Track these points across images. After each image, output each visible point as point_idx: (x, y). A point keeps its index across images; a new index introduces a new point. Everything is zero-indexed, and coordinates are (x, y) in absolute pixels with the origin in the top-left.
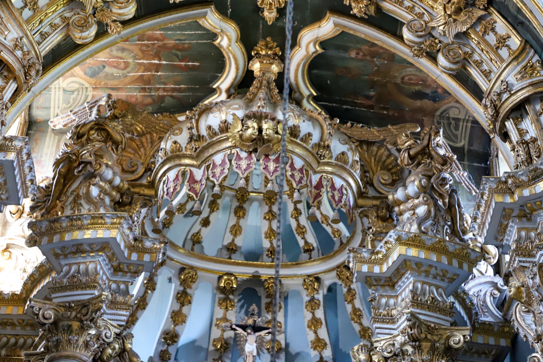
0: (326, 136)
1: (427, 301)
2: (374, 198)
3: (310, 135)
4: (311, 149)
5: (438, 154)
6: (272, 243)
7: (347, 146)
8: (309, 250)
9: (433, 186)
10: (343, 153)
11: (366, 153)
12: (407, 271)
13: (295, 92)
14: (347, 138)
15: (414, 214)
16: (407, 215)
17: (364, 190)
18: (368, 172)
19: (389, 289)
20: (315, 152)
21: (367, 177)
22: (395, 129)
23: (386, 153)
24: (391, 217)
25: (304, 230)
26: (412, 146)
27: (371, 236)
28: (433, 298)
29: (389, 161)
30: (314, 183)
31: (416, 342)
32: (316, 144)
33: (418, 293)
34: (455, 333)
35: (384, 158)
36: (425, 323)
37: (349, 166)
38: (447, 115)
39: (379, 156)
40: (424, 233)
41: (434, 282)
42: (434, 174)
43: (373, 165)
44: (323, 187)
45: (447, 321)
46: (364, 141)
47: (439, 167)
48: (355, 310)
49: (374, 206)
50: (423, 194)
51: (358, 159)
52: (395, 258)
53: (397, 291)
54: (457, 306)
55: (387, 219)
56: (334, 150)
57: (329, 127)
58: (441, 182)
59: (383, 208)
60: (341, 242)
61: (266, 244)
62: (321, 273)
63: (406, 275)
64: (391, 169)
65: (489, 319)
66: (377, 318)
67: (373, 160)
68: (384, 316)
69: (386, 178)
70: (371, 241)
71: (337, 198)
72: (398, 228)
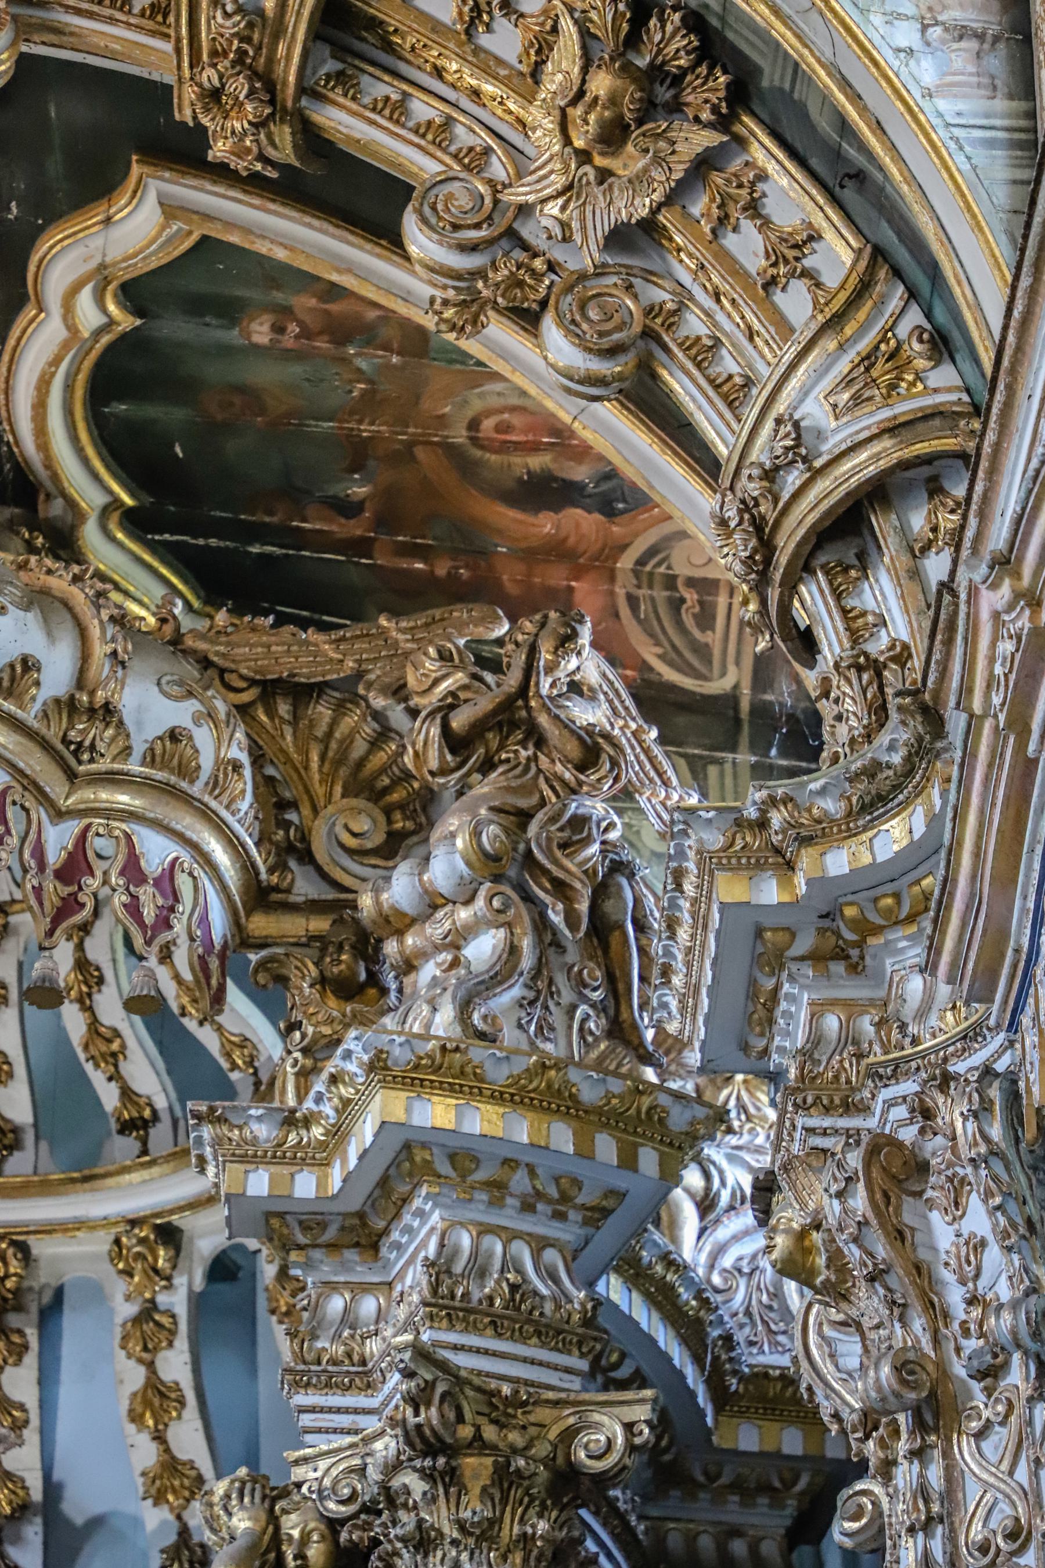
0: (100, 666)
1: (491, 1299)
2: (315, 907)
3: (28, 664)
4: (36, 725)
5: (567, 726)
7: (193, 705)
9: (529, 852)
10: (174, 735)
11: (288, 731)
12: (416, 1186)
13: (48, 496)
14: (190, 670)
15: (455, 963)
16: (429, 970)
17: (275, 879)
18: (294, 805)
19: (357, 1258)
20: (53, 733)
21: (286, 825)
22: (403, 631)
23: (369, 728)
24: (374, 979)
26: (462, 695)
27: (297, 1055)
28: (514, 1288)
29: (380, 758)
30: (54, 857)
31: (434, 1459)
32: (57, 701)
33: (458, 1268)
34: (596, 1417)
35: (360, 748)
36: (476, 1381)
37: (200, 784)
38: (662, 569)
39: (341, 742)
40: (482, 1036)
41: (526, 1224)
42: (543, 802)
43: (317, 777)
44: (92, 874)
45: (568, 1370)
46: (279, 680)
47: (567, 775)
49: (313, 938)
50: (489, 884)
51: (244, 758)
52: (369, 1139)
53: (387, 1266)
55: (361, 988)
56: (139, 724)
57: (111, 630)
58: (565, 834)
59: (340, 948)
60: (257, 1084)
63: (417, 1203)
64: (386, 791)
66: (303, 1373)
67: (315, 757)
68: (333, 1361)
69: (362, 824)
70: (297, 1075)
71: (149, 914)
72: (389, 1021)
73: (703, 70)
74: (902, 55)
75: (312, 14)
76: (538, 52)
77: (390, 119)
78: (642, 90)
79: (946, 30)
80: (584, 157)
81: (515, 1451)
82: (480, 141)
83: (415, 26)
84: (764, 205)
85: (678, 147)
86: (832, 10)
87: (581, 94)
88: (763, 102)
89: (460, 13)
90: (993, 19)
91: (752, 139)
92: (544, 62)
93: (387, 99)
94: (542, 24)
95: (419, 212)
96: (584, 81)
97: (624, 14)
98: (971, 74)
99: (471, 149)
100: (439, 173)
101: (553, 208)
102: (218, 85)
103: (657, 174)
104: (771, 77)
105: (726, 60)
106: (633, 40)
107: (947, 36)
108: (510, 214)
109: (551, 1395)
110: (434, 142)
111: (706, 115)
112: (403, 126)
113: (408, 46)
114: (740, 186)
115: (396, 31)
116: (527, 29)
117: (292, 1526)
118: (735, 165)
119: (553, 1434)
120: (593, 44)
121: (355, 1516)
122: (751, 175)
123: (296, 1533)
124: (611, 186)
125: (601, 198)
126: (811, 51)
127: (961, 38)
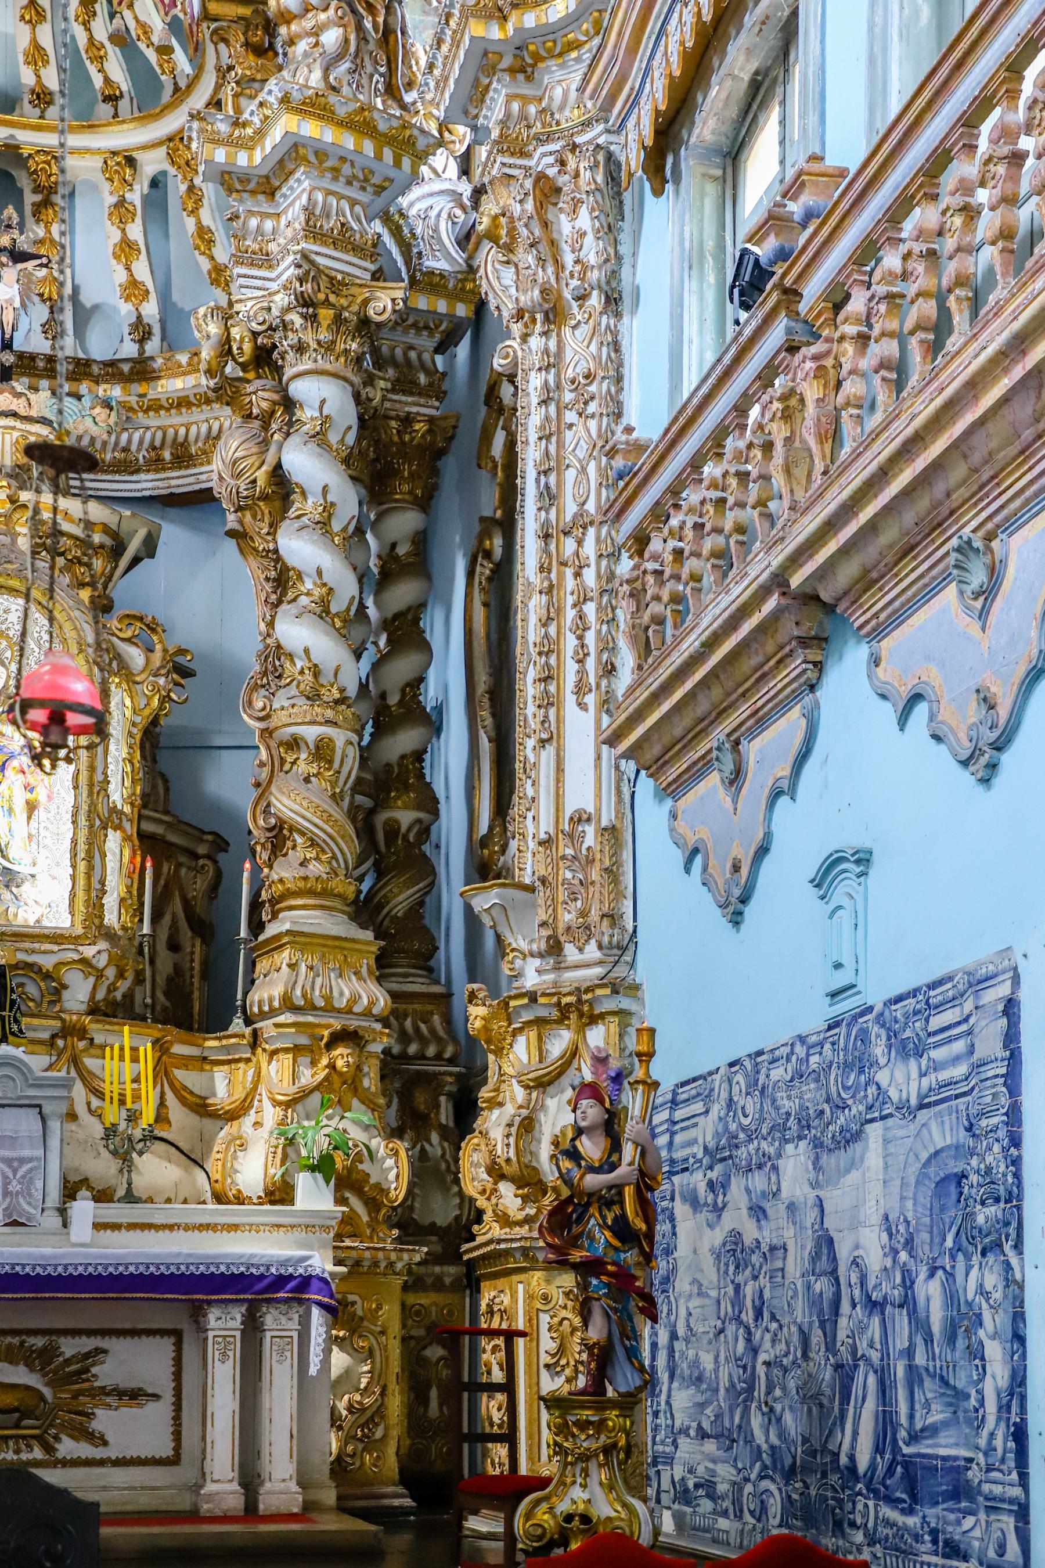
6: (38, 76)
8: (112, 98)
25: (102, 53)
34: (378, 294)
48: (202, 231)
54: (388, 240)
61: (28, 77)
62: (138, 149)
65: (441, 265)
81: (343, 308)
109: (358, 281)
117: (236, 333)
119: (359, 301)
121: (266, 331)
123: (238, 337)
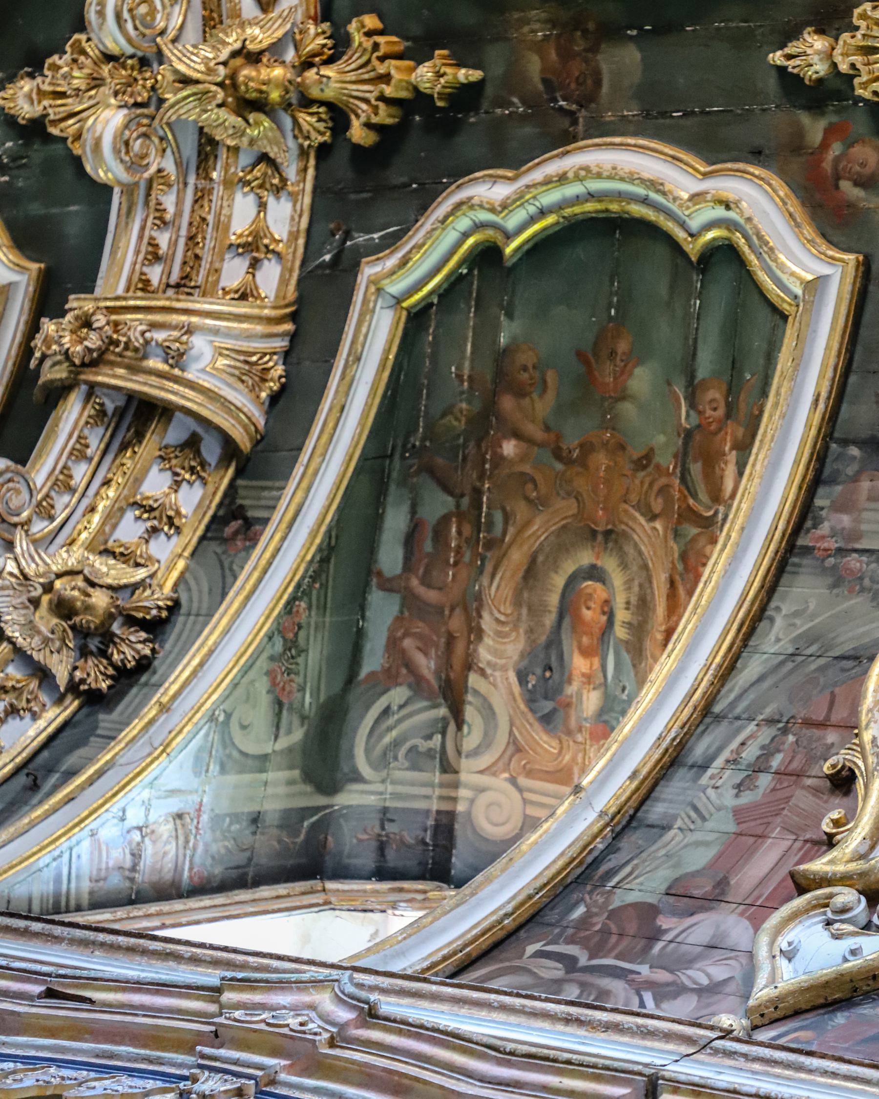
73: (111, 671)
74: (121, 814)
75: (145, 394)
76: (122, 554)
77: (73, 449)
78: (96, 628)
79: (138, 844)
80: (48, 588)
82: (58, 512)
83: (139, 466)
84: (14, 718)
85: (55, 655)
86: (152, 762)
87: (93, 585)
88: (88, 715)
89: (148, 498)
90: (146, 875)
91: (62, 708)
92: (115, 558)
93: (87, 446)
94: (141, 556)
95: (7, 470)
96: (101, 586)
97: (148, 613)
98: (107, 863)
99: (52, 507)
100: (35, 484)
101: (11, 567)
102: (95, 325)
103: (36, 641)
104: (105, 720)
105: (118, 686)
106: (131, 621)
107: (134, 845)
108: (7, 536)
110: (57, 480)
111: (78, 674)
112: (68, 458)
113: (124, 461)
114: (28, 701)
115: (135, 452)
116: (138, 545)
118: (44, 697)
120: (128, 592)
122: (36, 709)
124: (27, 608)
125: (19, 601)
126: (123, 749)
127: (133, 855)
